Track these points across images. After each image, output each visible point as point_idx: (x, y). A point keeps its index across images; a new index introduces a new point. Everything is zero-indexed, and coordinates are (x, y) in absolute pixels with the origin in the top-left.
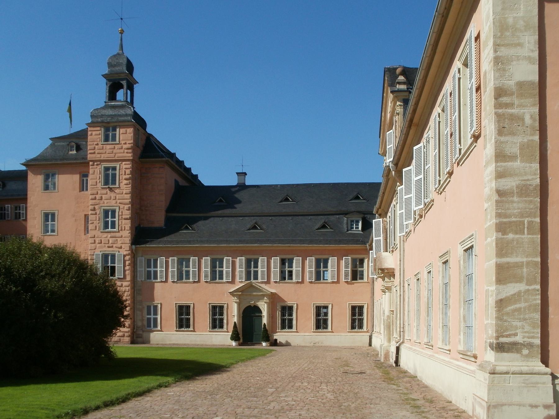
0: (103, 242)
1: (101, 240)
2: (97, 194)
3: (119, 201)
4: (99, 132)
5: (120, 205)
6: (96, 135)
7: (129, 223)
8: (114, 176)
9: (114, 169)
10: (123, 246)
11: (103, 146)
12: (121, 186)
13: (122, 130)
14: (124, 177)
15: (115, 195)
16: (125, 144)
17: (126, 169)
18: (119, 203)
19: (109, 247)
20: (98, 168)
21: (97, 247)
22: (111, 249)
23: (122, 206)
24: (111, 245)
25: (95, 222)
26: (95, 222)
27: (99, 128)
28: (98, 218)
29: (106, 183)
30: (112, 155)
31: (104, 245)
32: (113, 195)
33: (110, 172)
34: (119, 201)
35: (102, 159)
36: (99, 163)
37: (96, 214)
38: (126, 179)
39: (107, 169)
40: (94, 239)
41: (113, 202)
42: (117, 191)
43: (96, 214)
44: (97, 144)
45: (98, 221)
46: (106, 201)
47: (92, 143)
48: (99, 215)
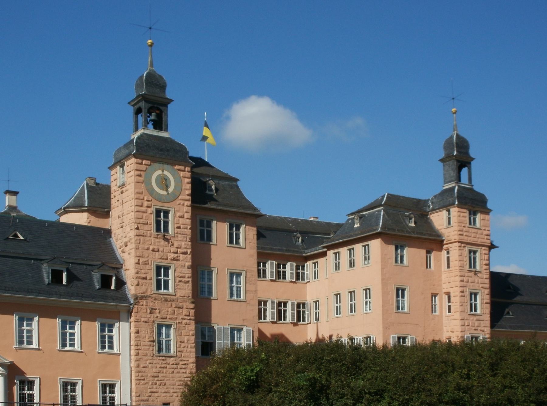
1: (469, 323)
3: (481, 285)
8: (475, 259)
10: (485, 329)
13: (483, 216)
14: (484, 263)
16: (485, 230)
17: (485, 254)
18: (482, 287)
19: (475, 330)
20: (465, 250)
21: (466, 329)
22: (476, 332)
23: (483, 290)
25: (464, 304)
27: (465, 210)
28: (466, 300)
30: (475, 239)
32: (476, 279)
34: (481, 285)
35: (468, 241)
36: (465, 245)
41: (476, 286)
42: (479, 275)
44: (464, 227)
45: (466, 304)
46: (471, 284)
47: (460, 224)
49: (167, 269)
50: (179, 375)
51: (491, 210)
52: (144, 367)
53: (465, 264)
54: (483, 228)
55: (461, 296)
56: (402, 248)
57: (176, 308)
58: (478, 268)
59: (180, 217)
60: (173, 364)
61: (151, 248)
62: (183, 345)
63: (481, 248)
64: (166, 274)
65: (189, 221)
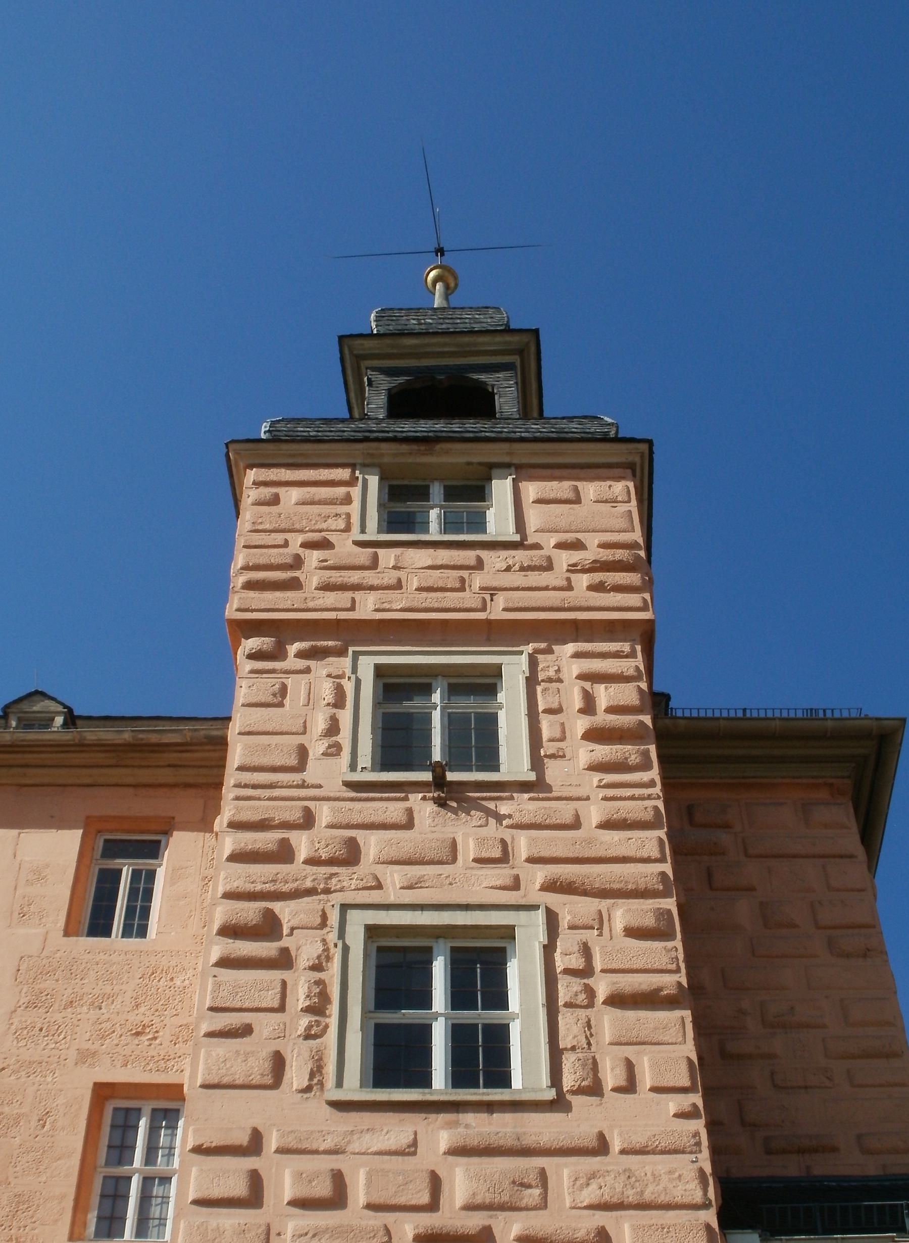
0: (359, 1194)
2: (308, 821)
4: (341, 491)
5: (553, 900)
7: (673, 1034)
11: (376, 554)
12: (549, 779)
15: (493, 830)
18: (551, 886)
25: (265, 1024)
26: (265, 1024)
31: (377, 1220)
34: (541, 874)
37: (284, 961)
40: (250, 1163)
43: (284, 961)
45: (305, 1021)
47: (279, 538)
48: (317, 967)
53: (317, 748)
55: (225, 962)
63: (549, 651)
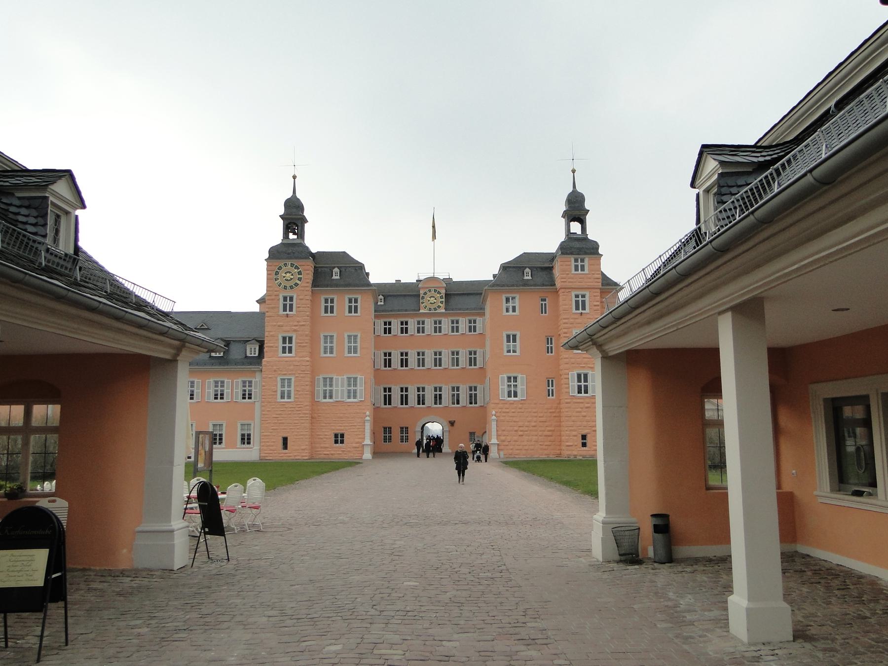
6: (566, 265)
8: (584, 302)
9: (583, 296)
24: (584, 366)
29: (577, 308)
31: (577, 365)
33: (580, 299)
38: (595, 306)
39: (577, 296)
42: (588, 316)
47: (564, 272)
49: (290, 339)
50: (296, 416)
51: (602, 255)
52: (268, 411)
54: (593, 272)
56: (513, 298)
57: (294, 366)
58: (587, 310)
59: (301, 299)
60: (291, 408)
61: (279, 324)
62: (300, 393)
64: (290, 341)
65: (309, 302)
